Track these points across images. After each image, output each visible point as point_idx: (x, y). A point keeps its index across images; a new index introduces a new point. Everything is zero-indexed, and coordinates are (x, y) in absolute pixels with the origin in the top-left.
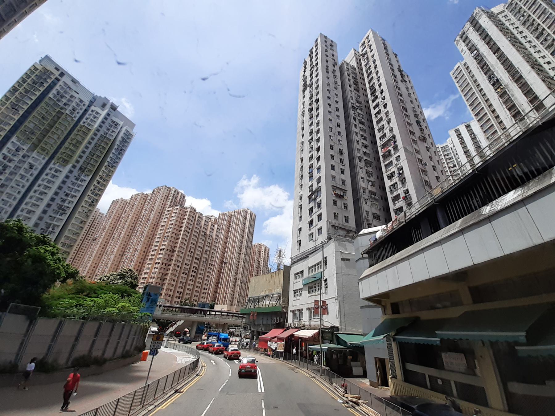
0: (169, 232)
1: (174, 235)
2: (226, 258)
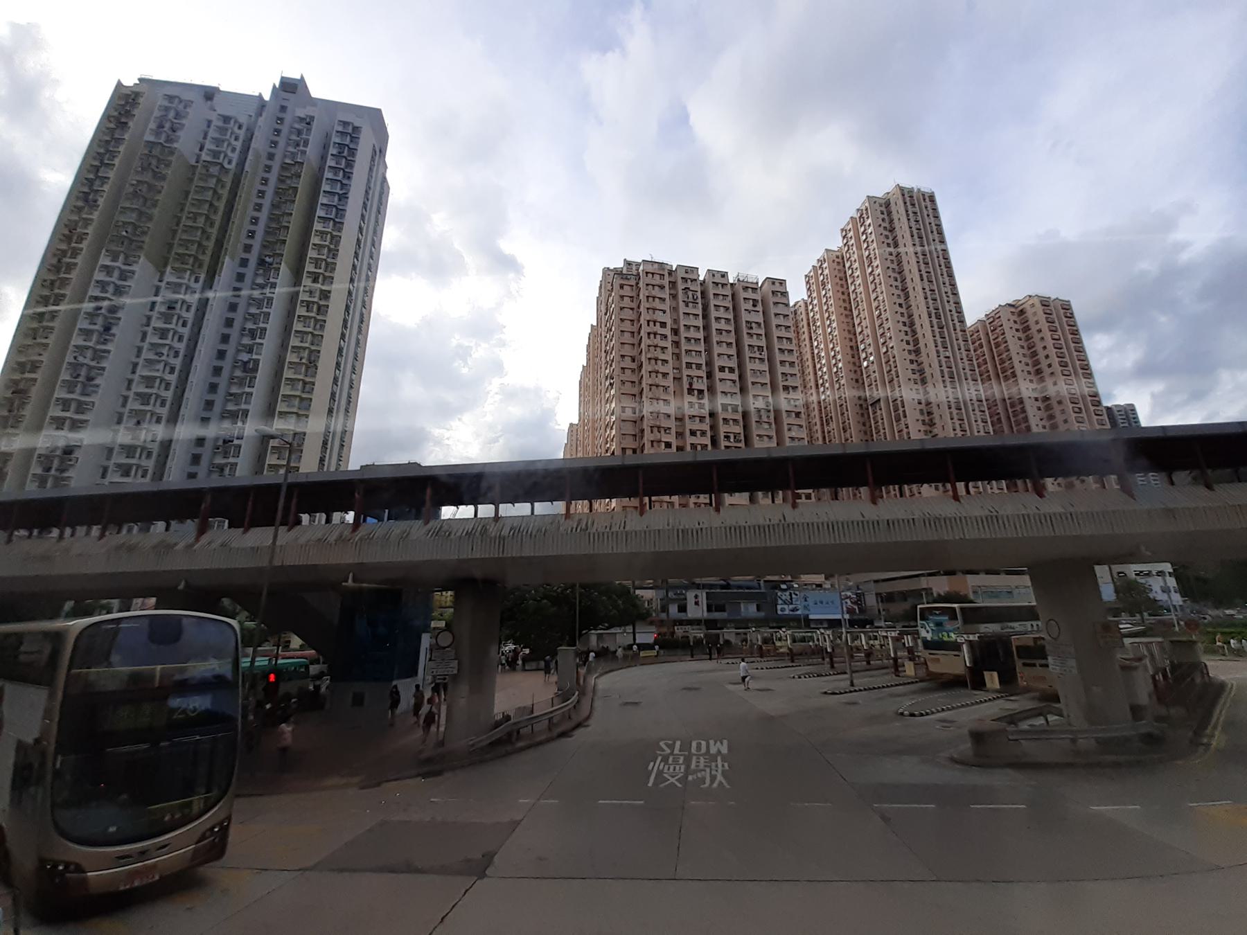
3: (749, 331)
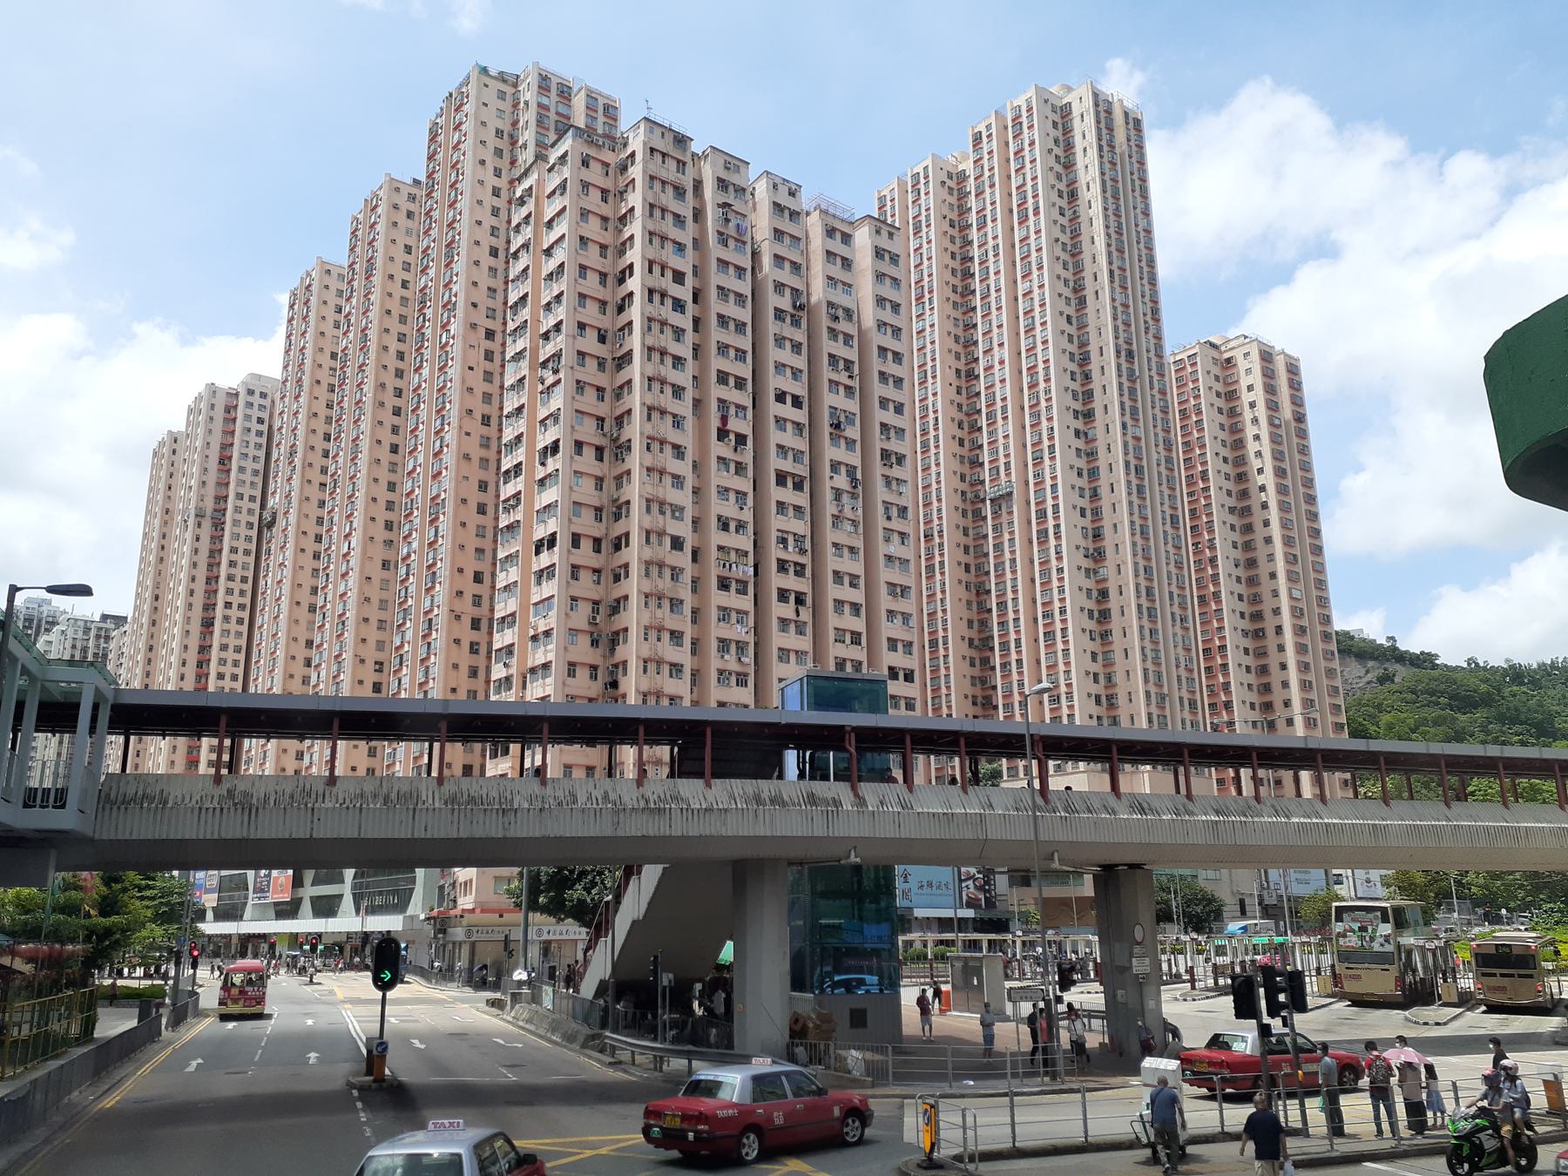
0: (557, 327)
1: (590, 343)
2: (995, 470)
3: (833, 325)
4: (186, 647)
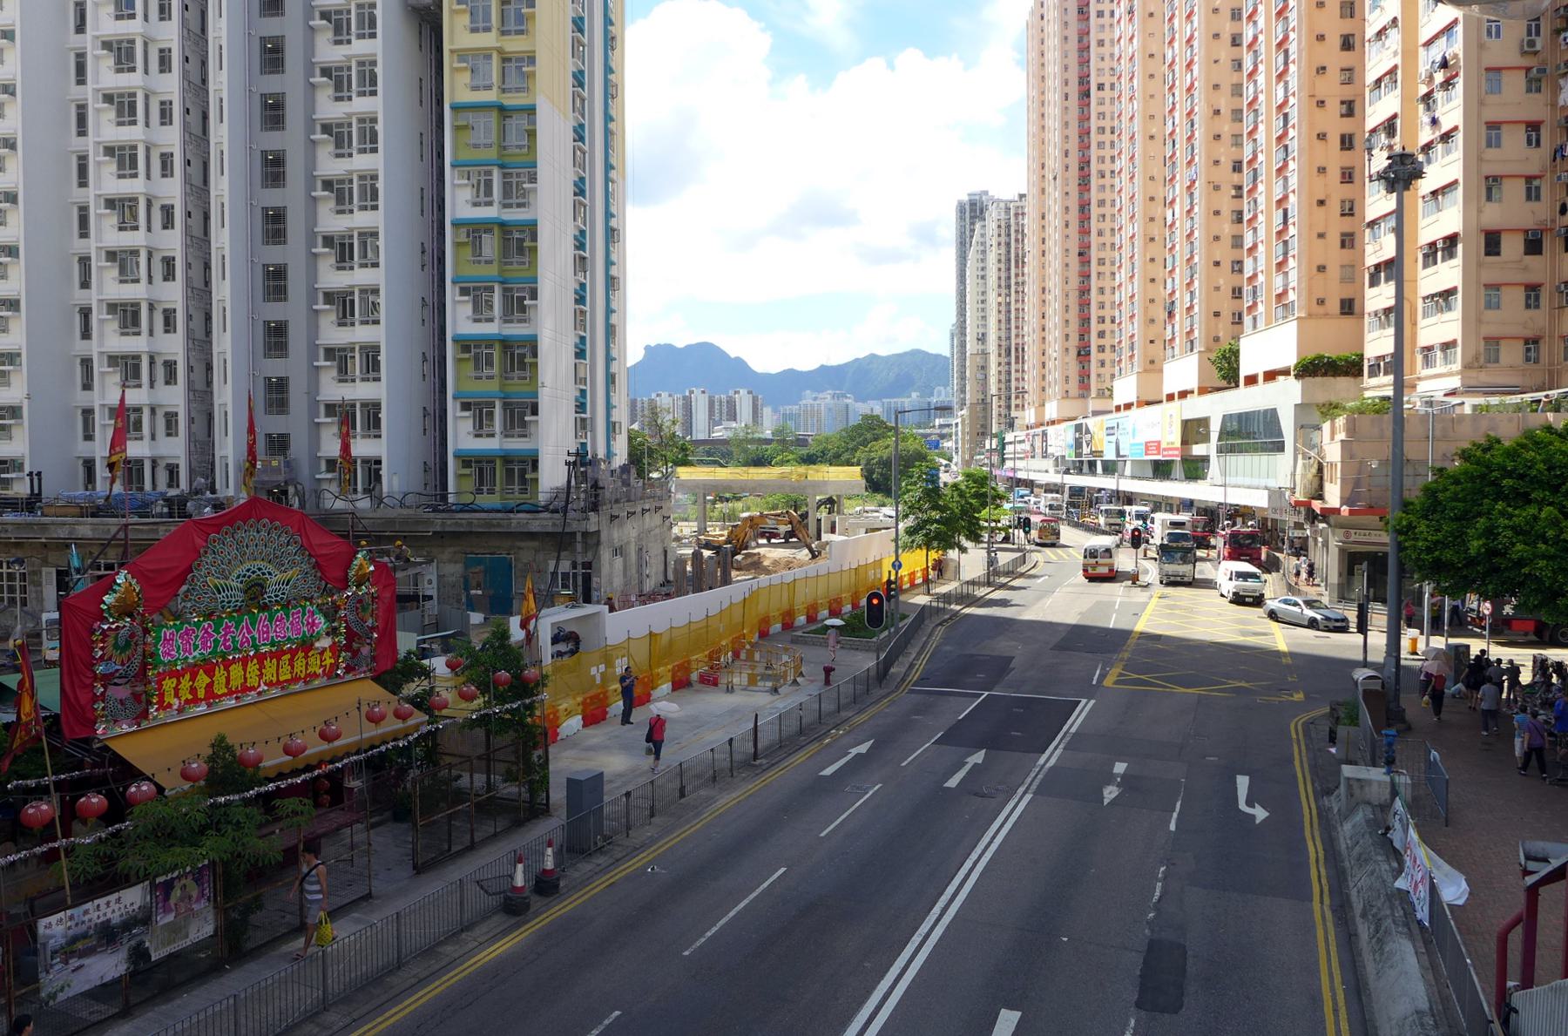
4: (1067, 208)
